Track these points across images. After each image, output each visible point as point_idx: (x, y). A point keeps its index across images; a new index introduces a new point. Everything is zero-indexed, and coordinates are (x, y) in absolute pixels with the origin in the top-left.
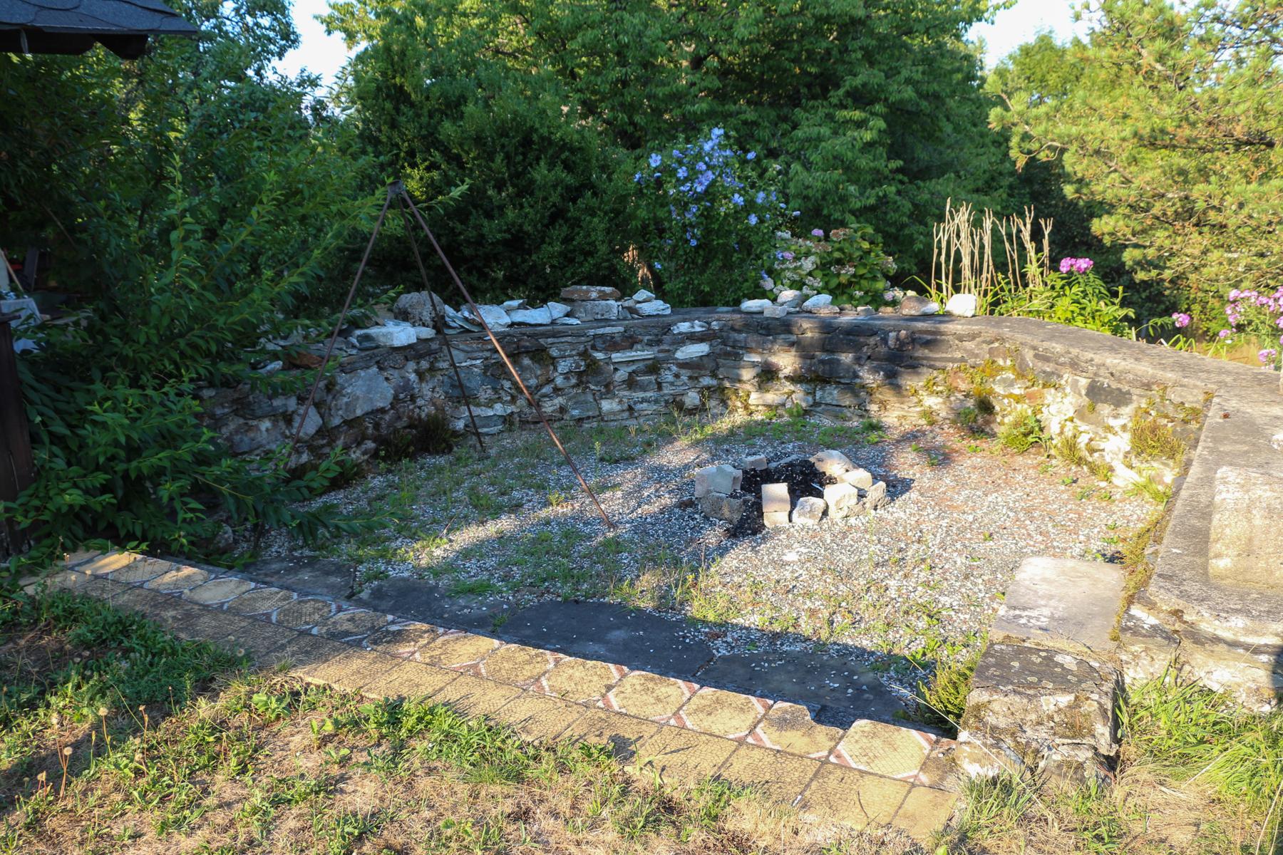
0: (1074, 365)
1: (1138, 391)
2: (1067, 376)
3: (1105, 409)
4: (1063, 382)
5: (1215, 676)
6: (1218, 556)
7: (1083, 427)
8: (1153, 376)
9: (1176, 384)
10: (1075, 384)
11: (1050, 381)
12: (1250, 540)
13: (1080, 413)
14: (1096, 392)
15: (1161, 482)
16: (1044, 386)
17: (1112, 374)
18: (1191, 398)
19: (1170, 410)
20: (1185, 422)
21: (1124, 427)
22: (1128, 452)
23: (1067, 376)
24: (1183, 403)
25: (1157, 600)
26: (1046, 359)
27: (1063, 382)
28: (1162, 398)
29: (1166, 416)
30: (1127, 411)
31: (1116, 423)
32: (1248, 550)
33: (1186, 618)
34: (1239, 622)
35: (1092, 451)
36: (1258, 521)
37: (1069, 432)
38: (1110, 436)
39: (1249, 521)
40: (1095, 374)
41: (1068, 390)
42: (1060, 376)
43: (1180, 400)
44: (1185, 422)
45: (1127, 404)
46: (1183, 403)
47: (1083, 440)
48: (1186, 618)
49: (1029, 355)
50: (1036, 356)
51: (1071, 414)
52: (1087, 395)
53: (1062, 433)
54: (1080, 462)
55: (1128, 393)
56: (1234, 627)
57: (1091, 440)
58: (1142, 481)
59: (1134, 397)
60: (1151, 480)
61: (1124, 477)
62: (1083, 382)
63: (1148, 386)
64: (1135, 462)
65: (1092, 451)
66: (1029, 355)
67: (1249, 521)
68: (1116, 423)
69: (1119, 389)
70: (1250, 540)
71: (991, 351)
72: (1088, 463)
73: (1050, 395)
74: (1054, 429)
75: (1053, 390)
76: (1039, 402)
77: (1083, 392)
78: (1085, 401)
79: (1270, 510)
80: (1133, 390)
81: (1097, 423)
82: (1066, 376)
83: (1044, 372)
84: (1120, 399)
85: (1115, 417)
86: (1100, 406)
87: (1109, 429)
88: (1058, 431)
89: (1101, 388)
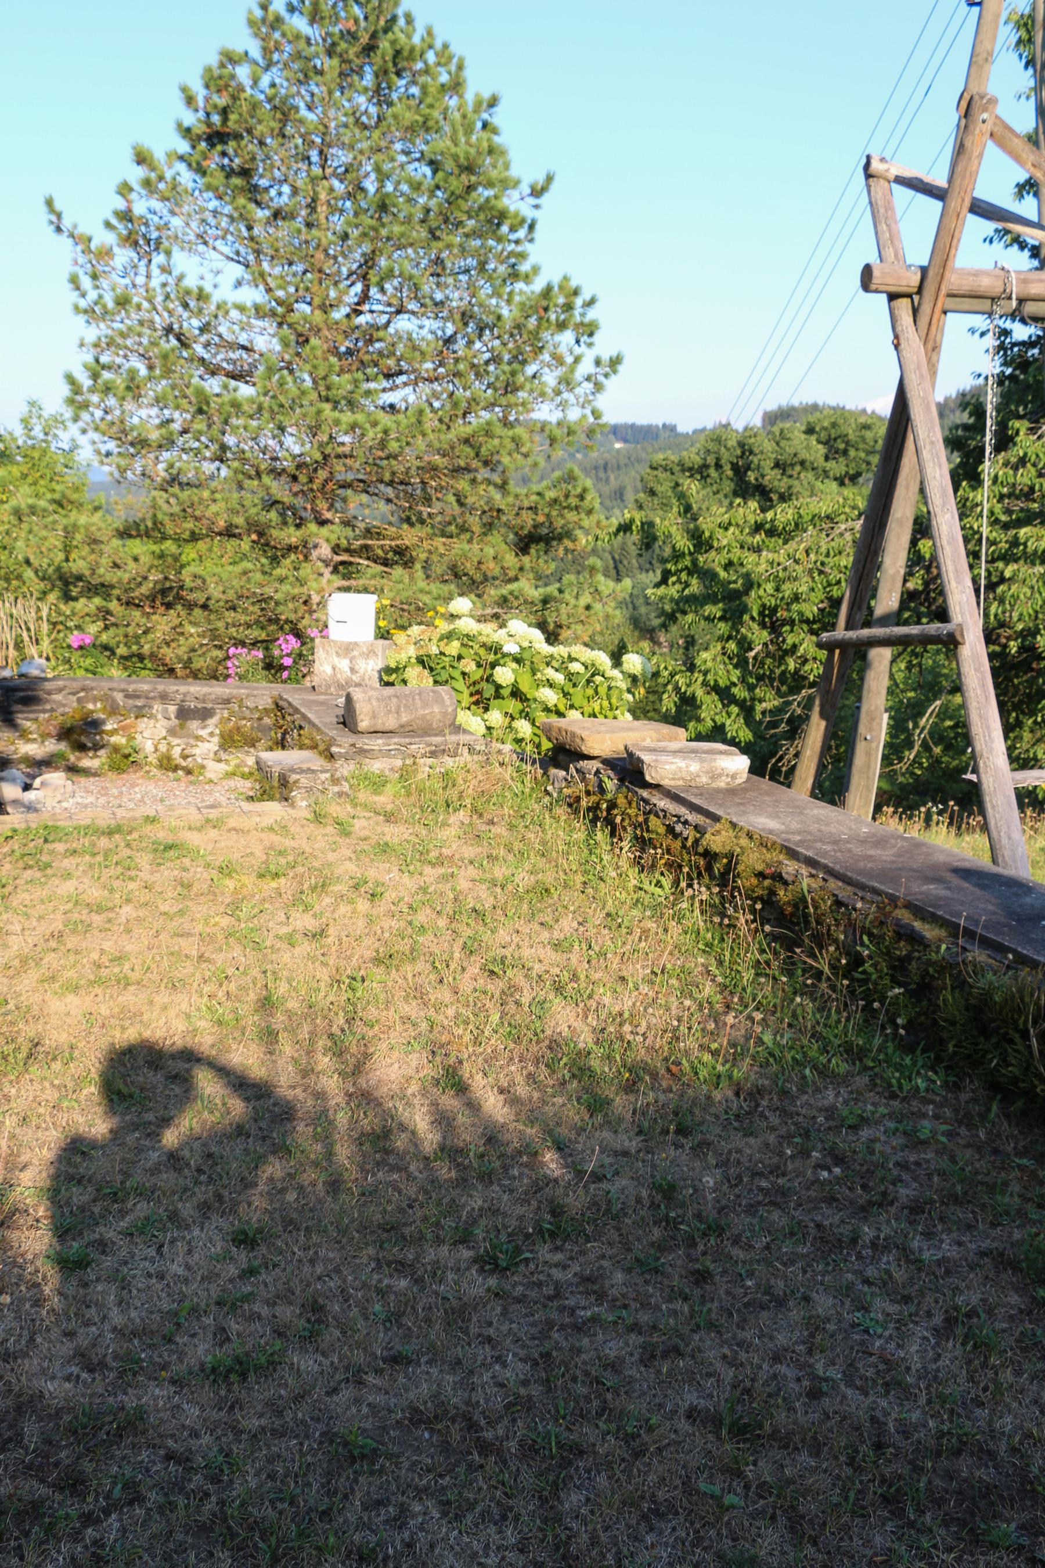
0: (164, 697)
2: (157, 707)
3: (194, 725)
7: (175, 741)
11: (140, 713)
13: (172, 732)
14: (184, 714)
19: (248, 714)
20: (260, 719)
21: (212, 734)
23: (157, 707)
26: (138, 697)
30: (212, 721)
31: (204, 733)
32: (374, 716)
35: (185, 757)
37: (163, 748)
42: (151, 707)
44: (260, 719)
47: (176, 752)
49: (119, 697)
50: (127, 696)
51: (164, 733)
54: (176, 768)
56: (377, 743)
58: (230, 769)
60: (238, 766)
61: (215, 769)
62: (172, 709)
63: (227, 701)
64: (223, 756)
65: (185, 757)
66: (119, 697)
68: (204, 733)
71: (79, 700)
72: (183, 768)
73: (143, 724)
74: (149, 747)
78: (175, 722)
81: (188, 736)
84: (205, 714)
87: (198, 738)
89: (189, 709)
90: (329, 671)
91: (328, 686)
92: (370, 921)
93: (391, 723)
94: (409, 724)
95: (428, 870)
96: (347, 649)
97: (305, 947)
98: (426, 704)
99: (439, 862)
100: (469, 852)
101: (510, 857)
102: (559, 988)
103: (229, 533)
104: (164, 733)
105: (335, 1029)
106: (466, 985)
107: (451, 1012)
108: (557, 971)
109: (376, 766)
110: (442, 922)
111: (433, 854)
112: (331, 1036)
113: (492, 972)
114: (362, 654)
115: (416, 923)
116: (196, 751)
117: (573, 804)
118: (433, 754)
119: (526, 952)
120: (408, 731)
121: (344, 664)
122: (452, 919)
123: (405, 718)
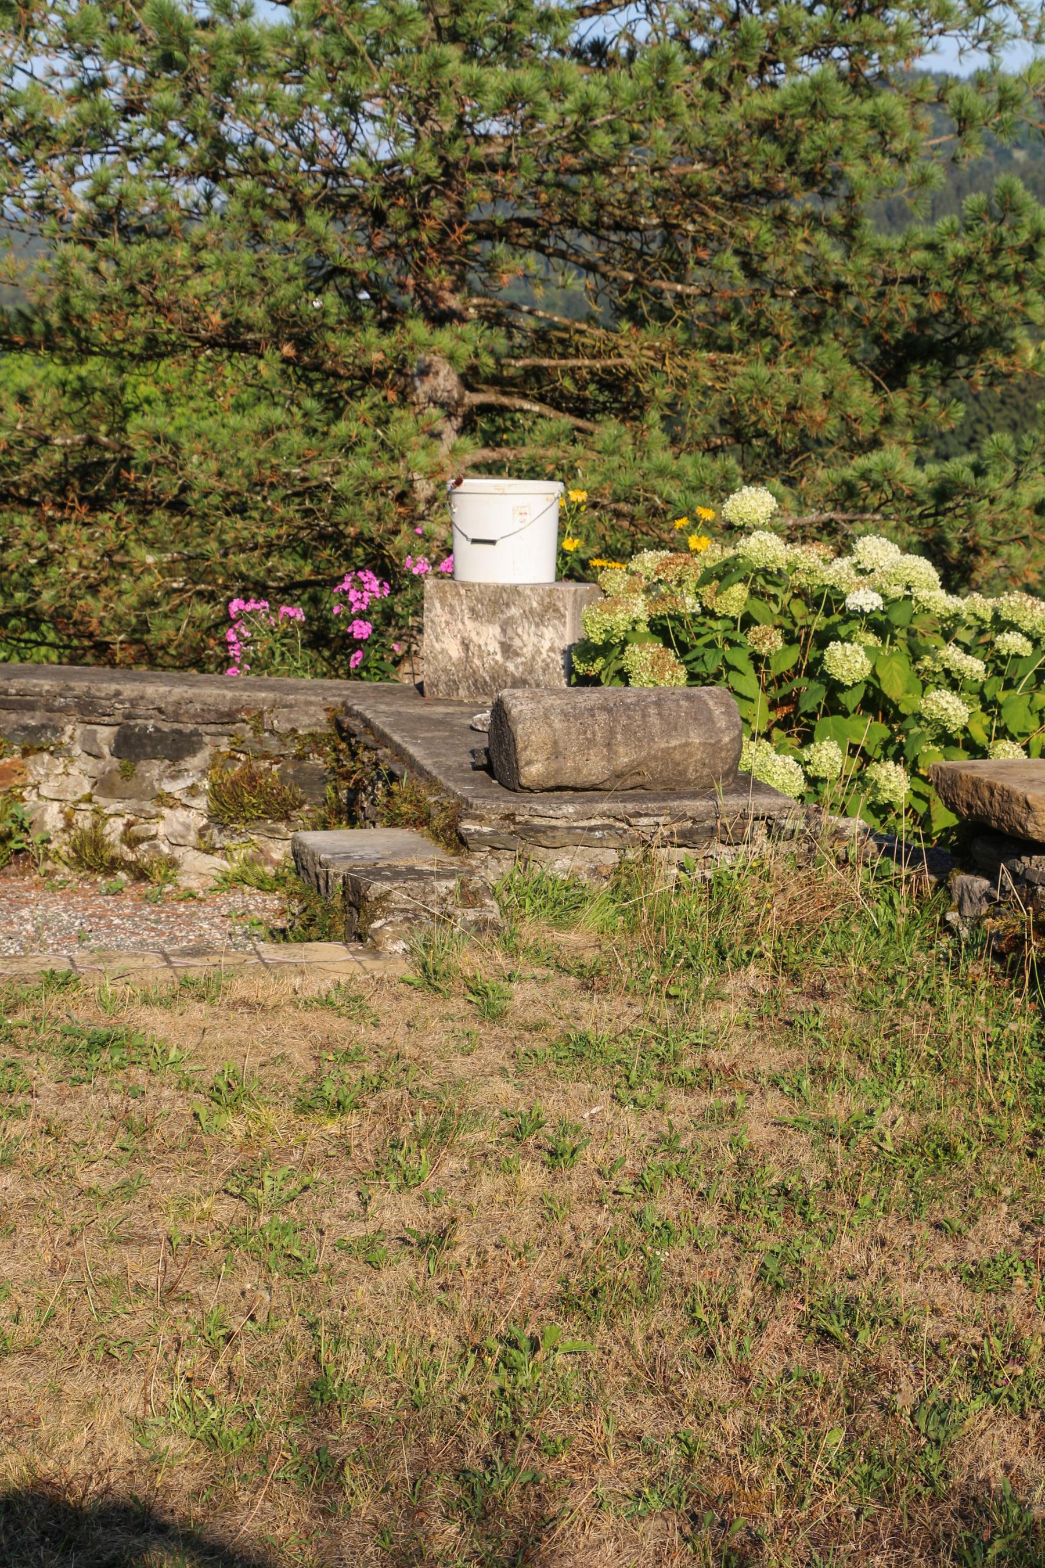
0: (88, 709)
1: (212, 728)
2: (72, 730)
3: (153, 770)
4: (65, 739)
5: (558, 865)
6: (529, 763)
7: (113, 806)
8: (235, 700)
9: (274, 706)
10: (90, 738)
12: (555, 743)
13: (104, 785)
14: (132, 745)
15: (269, 861)
16: (26, 753)
17: (160, 710)
18: (306, 720)
19: (273, 745)
20: (300, 758)
21: (193, 791)
22: (206, 827)
23: (72, 730)
24: (294, 730)
25: (484, 812)
26: (31, 707)
27: (65, 739)
28: (255, 730)
29: (266, 756)
30: (195, 762)
31: (175, 788)
32: (556, 753)
33: (518, 819)
34: (570, 809)
35: (132, 841)
36: (558, 725)
37: (84, 821)
38: (166, 811)
39: (550, 726)
40: (129, 717)
41: (77, 750)
42: (58, 730)
43: (289, 727)
44: (300, 758)
45: (193, 751)
46: (294, 730)
48: (518, 819)
52: (116, 753)
53: (69, 825)
54: (112, 866)
55: (195, 733)
56: (566, 812)
57: (129, 825)
59: (207, 739)
60: (250, 862)
61: (199, 869)
62: (105, 734)
63: (228, 717)
64: (219, 839)
67: (550, 726)
68: (175, 788)
69: (179, 732)
70: (555, 743)
72: (128, 866)
73: (39, 766)
74: (53, 817)
75: (46, 757)
76: (17, 781)
77: (106, 750)
79: (565, 715)
80: (202, 729)
81: (140, 795)
82: (69, 729)
83: (25, 728)
84: (177, 747)
85: (174, 777)
86: (143, 765)
87: (164, 799)
88: (61, 825)
90: (455, 651)
91: (453, 685)
92: (549, 1212)
93: (594, 767)
94: (634, 770)
95: (677, 1099)
96: (496, 602)
97: (404, 1270)
98: (671, 727)
99: (704, 1081)
100: (769, 1059)
101: (863, 1073)
102: (980, 1376)
103: (233, 340)
104: (87, 789)
105: (471, 1460)
106: (766, 1365)
107: (731, 1424)
108: (973, 1334)
109: (562, 864)
110: (710, 1218)
111: (688, 1064)
112: (462, 1474)
113: (825, 1335)
114: (528, 615)
115: (652, 1219)
116: (160, 828)
117: (1006, 954)
118: (687, 839)
119: (904, 1291)
120: (633, 786)
121: (488, 637)
122: (732, 1211)
123: (624, 758)
